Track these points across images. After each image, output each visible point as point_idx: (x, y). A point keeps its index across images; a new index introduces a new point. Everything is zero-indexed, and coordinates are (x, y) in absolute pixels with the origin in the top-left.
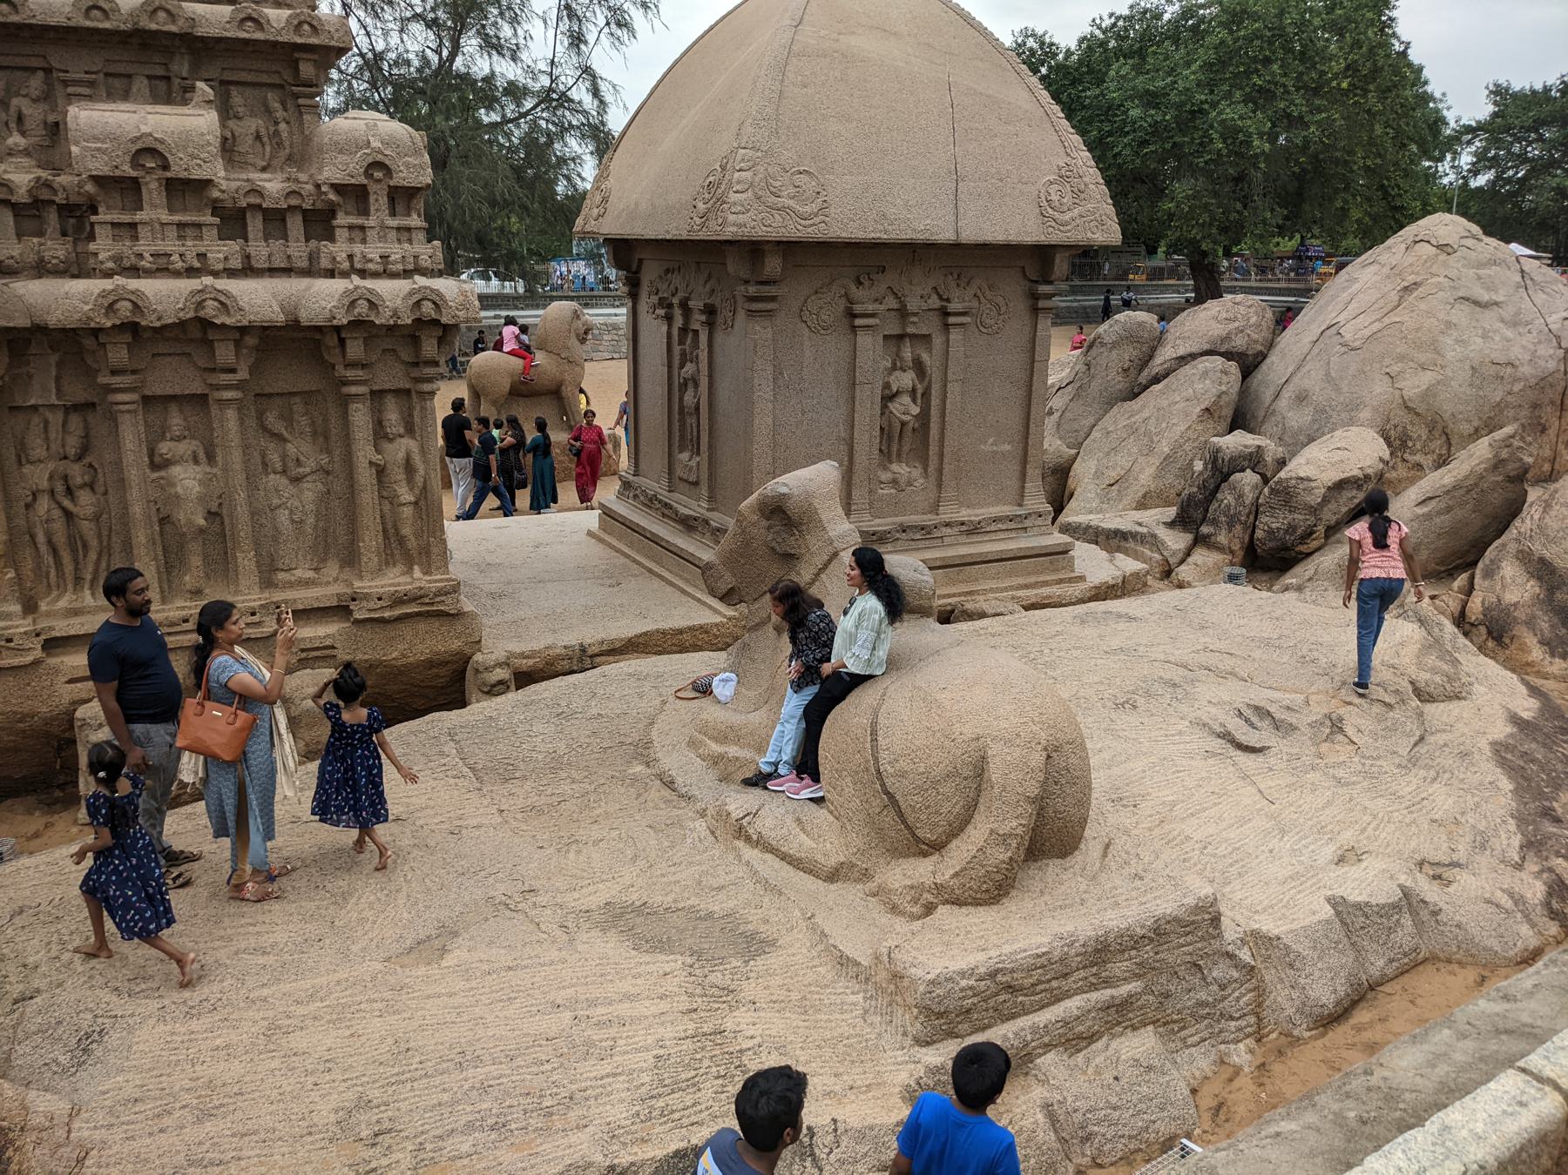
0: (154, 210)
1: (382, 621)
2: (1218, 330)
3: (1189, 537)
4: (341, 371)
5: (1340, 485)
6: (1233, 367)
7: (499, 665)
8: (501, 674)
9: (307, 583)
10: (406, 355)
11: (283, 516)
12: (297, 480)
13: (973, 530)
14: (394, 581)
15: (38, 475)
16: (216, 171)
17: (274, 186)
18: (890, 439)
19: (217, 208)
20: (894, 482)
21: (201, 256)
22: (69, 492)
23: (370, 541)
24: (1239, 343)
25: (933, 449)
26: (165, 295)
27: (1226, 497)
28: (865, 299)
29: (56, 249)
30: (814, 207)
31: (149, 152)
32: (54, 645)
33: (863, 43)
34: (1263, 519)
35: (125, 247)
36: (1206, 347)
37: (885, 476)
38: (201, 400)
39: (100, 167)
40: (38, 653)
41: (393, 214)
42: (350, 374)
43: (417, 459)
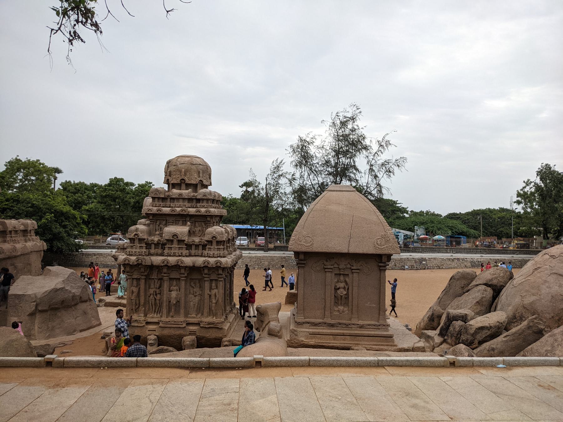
0: (175, 245)
1: (205, 327)
2: (489, 277)
3: (442, 339)
4: (204, 275)
5: (482, 328)
6: (489, 289)
7: (226, 341)
8: (226, 343)
9: (194, 318)
10: (216, 273)
11: (192, 303)
12: (195, 296)
13: (361, 327)
14: (210, 319)
15: (152, 291)
16: (186, 238)
17: (197, 240)
18: (338, 299)
19: (186, 245)
20: (339, 311)
21: (182, 253)
22: (156, 295)
23: (206, 310)
24: (495, 282)
25: (350, 304)
26: (172, 260)
27: (451, 328)
28: (329, 265)
29: (160, 251)
30: (309, 244)
31: (175, 235)
32: (148, 323)
33: (333, 207)
34: (462, 336)
35: (169, 251)
36: (485, 282)
37: (336, 309)
38: (179, 279)
39: (167, 238)
40: (144, 324)
41: (217, 245)
42: (205, 276)
43: (217, 294)
